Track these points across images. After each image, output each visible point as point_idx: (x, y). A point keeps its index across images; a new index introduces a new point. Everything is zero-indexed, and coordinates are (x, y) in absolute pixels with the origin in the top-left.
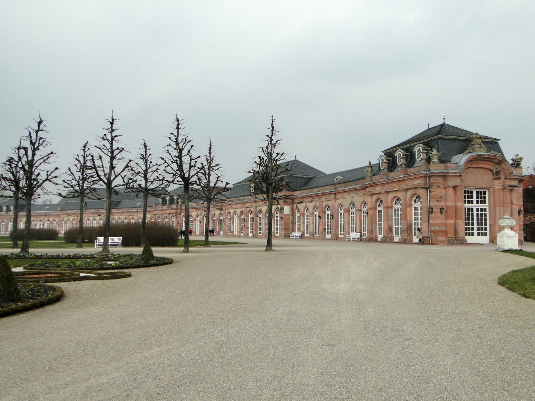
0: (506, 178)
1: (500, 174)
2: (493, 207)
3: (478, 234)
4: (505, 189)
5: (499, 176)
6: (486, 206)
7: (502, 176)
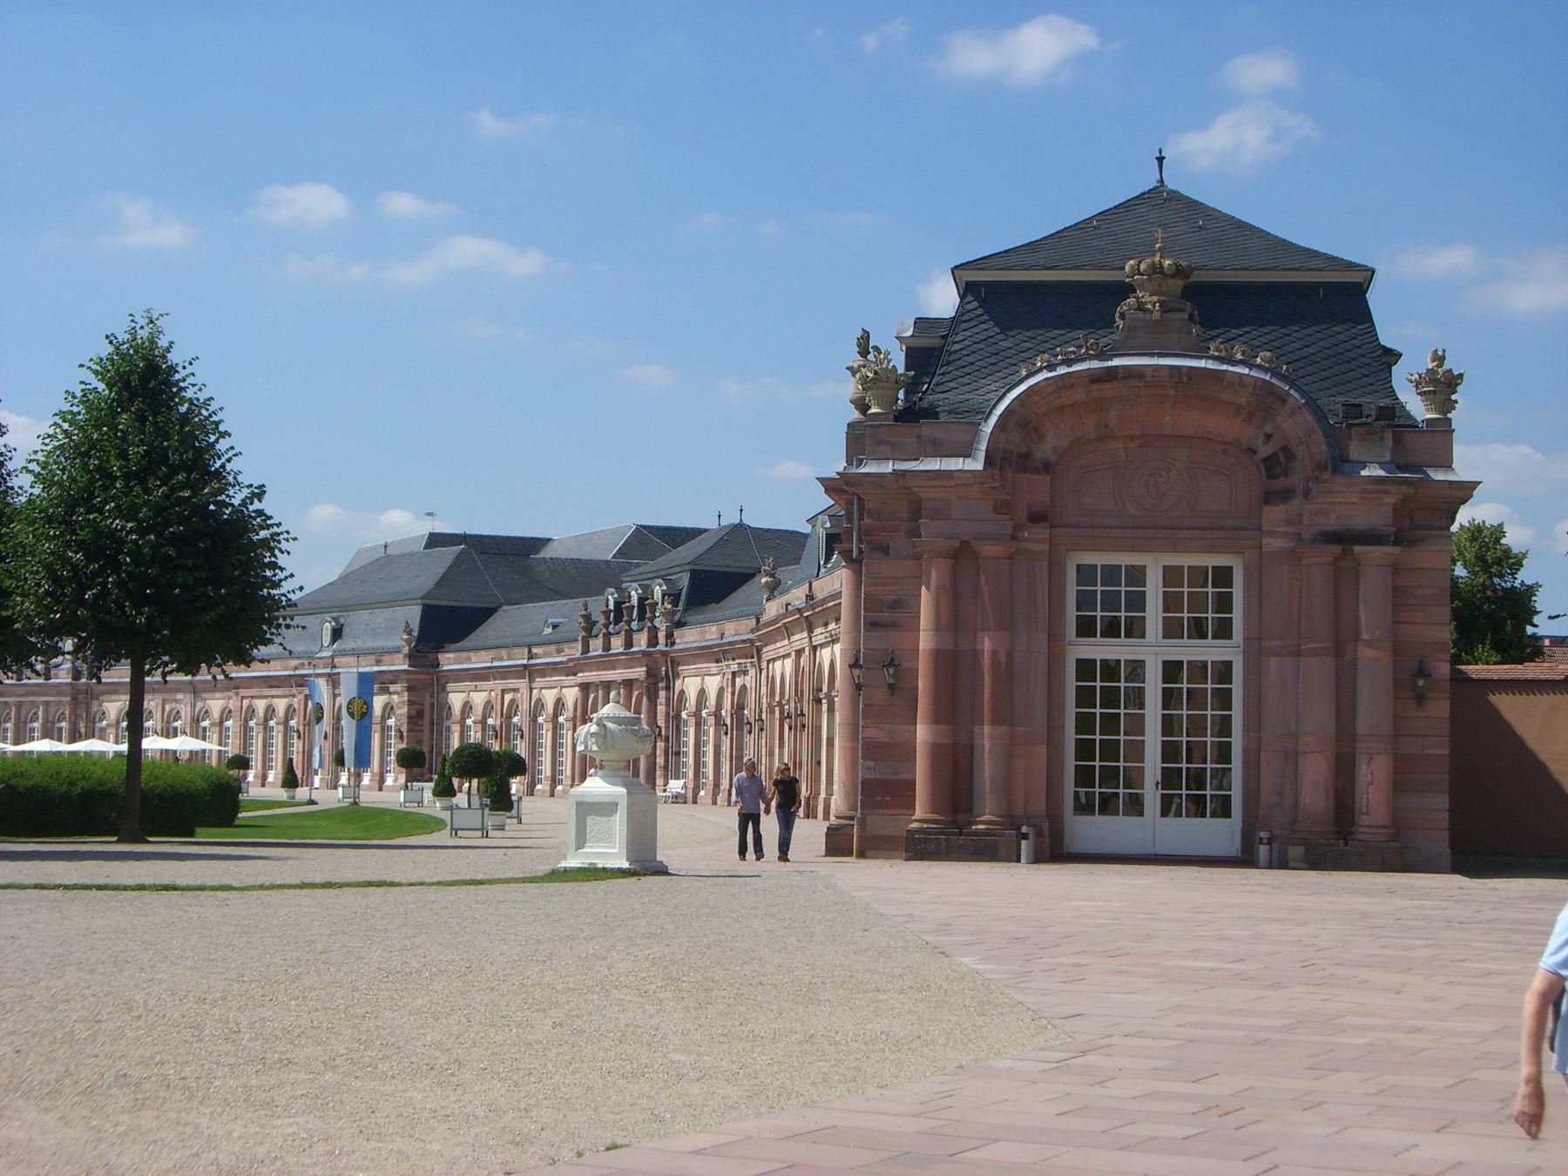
1: (1286, 473)
2: (1255, 652)
3: (1166, 808)
5: (1283, 478)
6: (1228, 651)
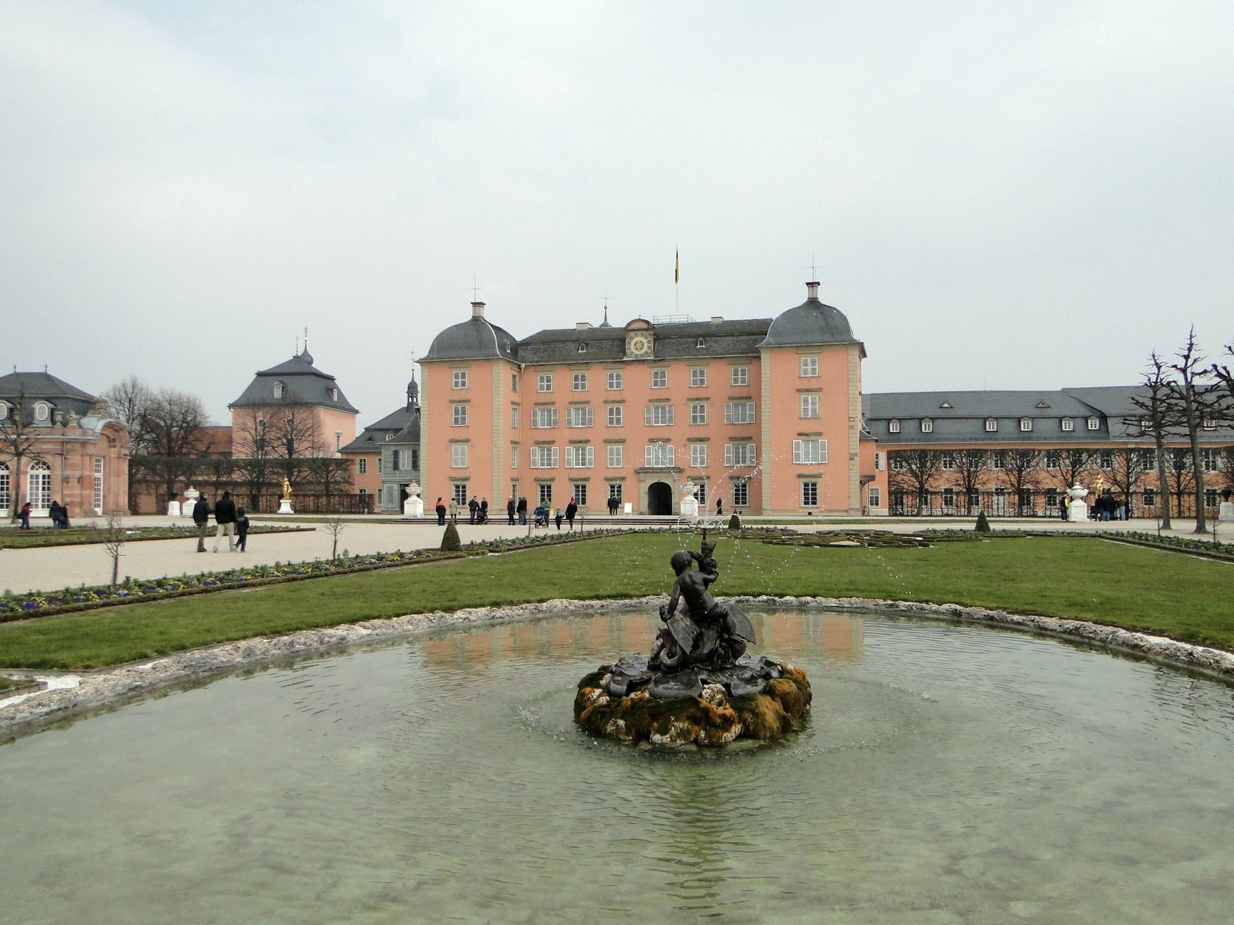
0: (121, 447)
4: (121, 458)
7: (118, 445)
